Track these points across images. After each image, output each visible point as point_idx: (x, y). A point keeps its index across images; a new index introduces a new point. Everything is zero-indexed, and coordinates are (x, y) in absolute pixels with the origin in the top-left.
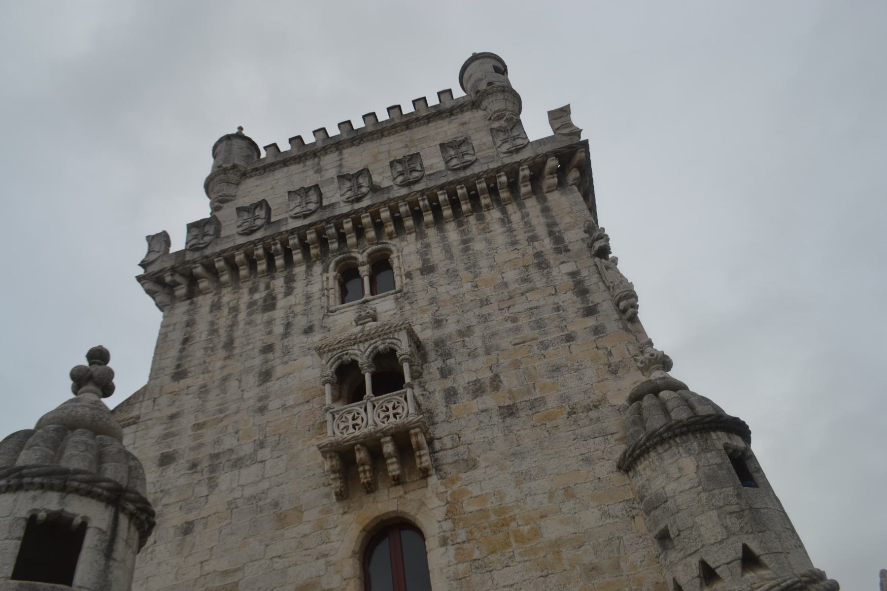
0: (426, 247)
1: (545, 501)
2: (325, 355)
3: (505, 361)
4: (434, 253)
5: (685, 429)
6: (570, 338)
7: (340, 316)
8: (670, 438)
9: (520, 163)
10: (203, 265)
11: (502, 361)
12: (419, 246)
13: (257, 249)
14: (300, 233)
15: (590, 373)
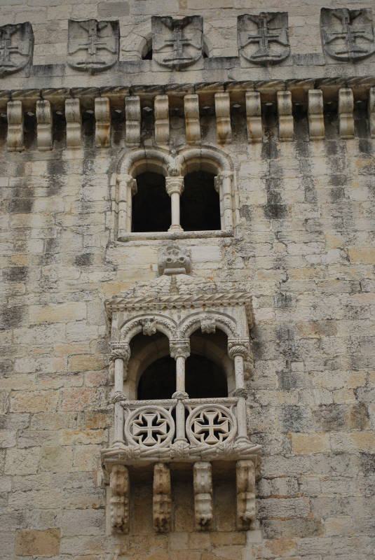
2: (118, 314)
4: (288, 187)
7: (134, 249)
12: (265, 168)
13: (12, 106)
14: (87, 100)
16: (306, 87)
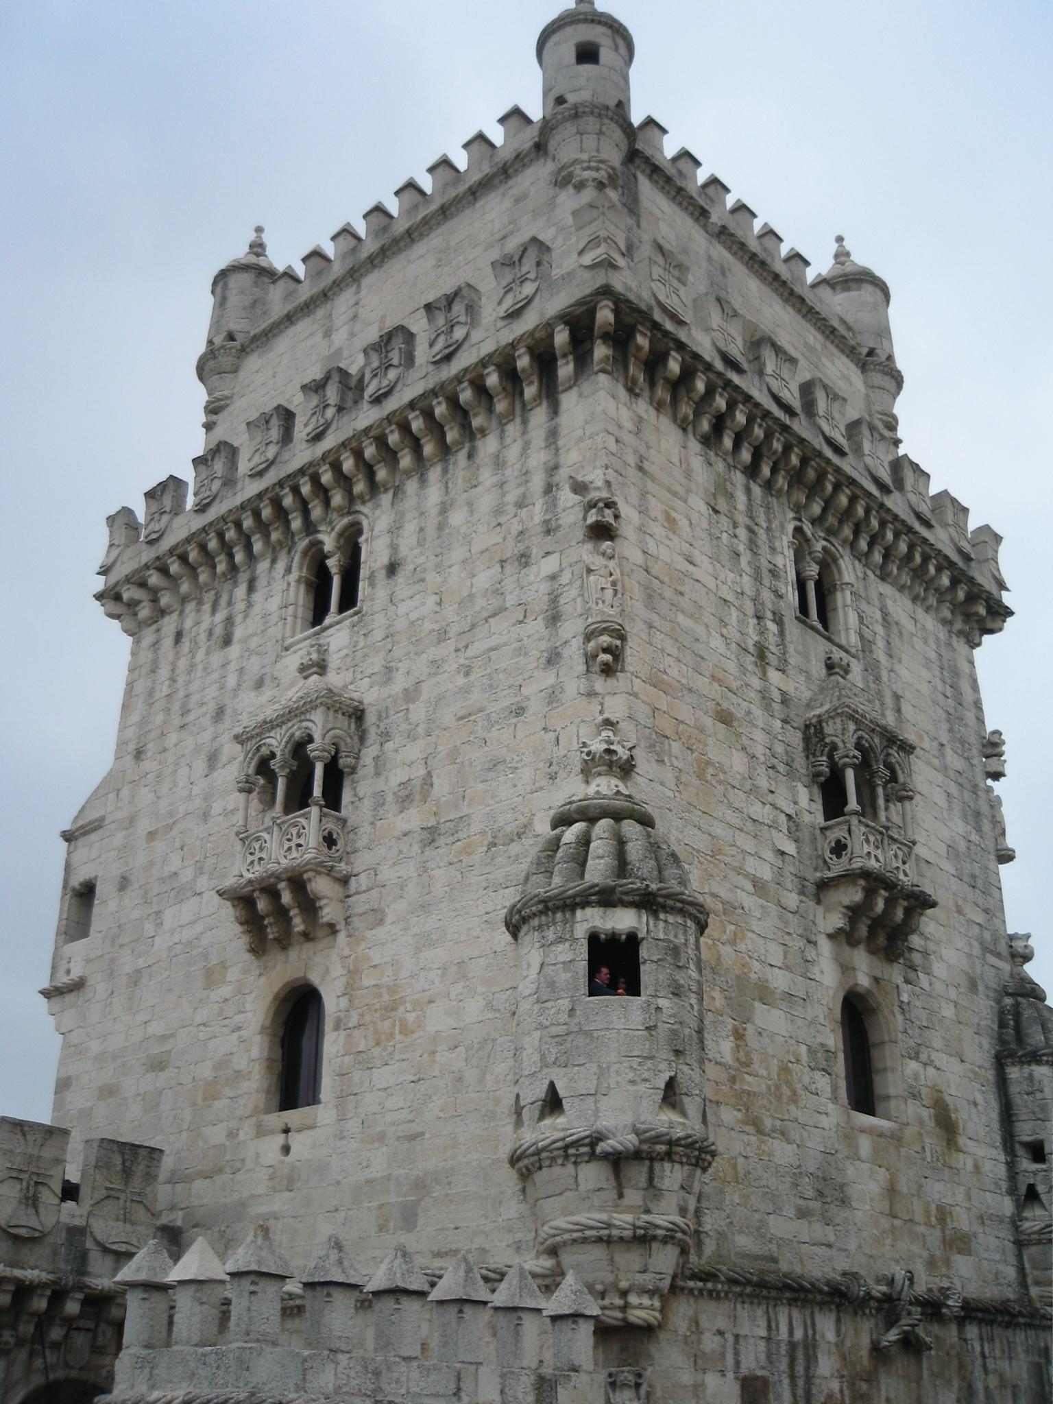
6: (520, 711)
9: (513, 346)
11: (440, 748)
14: (251, 507)
15: (526, 774)
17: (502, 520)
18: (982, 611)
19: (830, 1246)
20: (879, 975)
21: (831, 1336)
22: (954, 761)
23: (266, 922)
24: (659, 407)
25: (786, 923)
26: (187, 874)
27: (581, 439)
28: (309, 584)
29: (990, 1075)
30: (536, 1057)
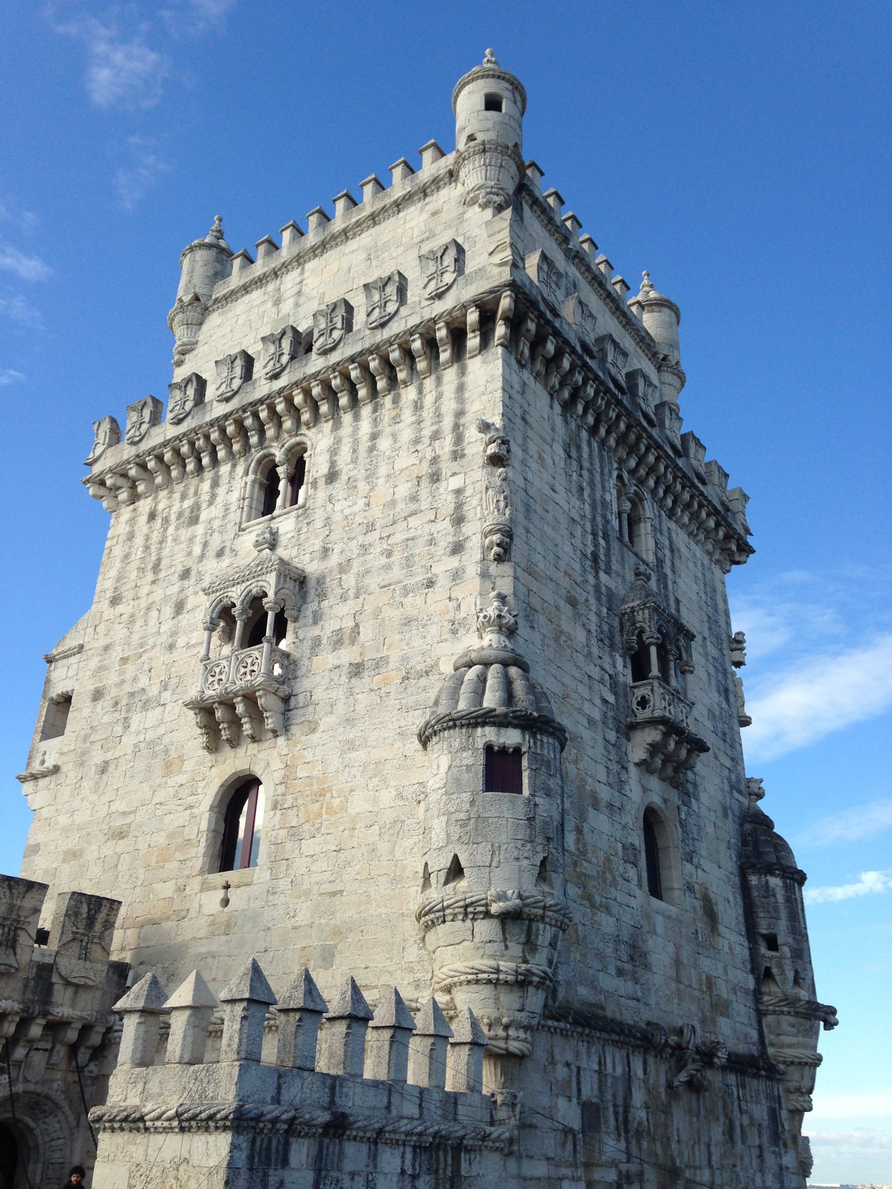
0: (337, 443)
1: (358, 774)
3: (369, 608)
4: (343, 453)
5: (451, 723)
6: (430, 584)
8: (440, 731)
9: (434, 321)
10: (137, 464)
11: (366, 608)
15: (434, 630)
16: (346, 365)
17: (419, 447)
18: (734, 547)
19: (638, 1000)
20: (666, 797)
21: (640, 1073)
22: (712, 651)
23: (221, 727)
24: (537, 376)
25: (609, 751)
26: (154, 691)
27: (483, 394)
28: (261, 485)
29: (737, 880)
30: (443, 836)
